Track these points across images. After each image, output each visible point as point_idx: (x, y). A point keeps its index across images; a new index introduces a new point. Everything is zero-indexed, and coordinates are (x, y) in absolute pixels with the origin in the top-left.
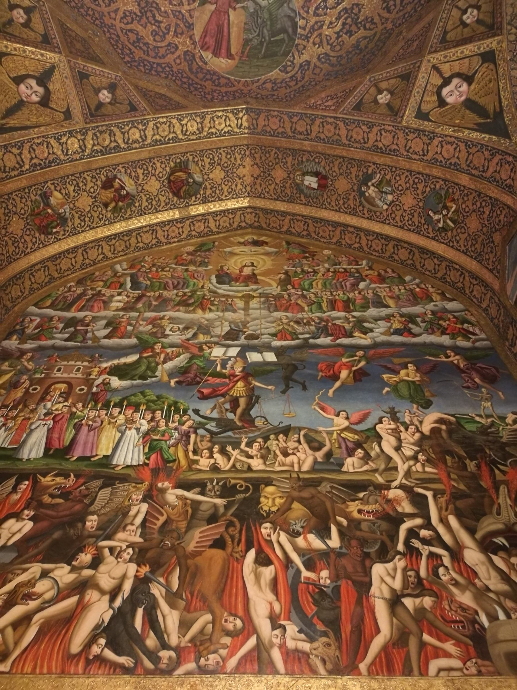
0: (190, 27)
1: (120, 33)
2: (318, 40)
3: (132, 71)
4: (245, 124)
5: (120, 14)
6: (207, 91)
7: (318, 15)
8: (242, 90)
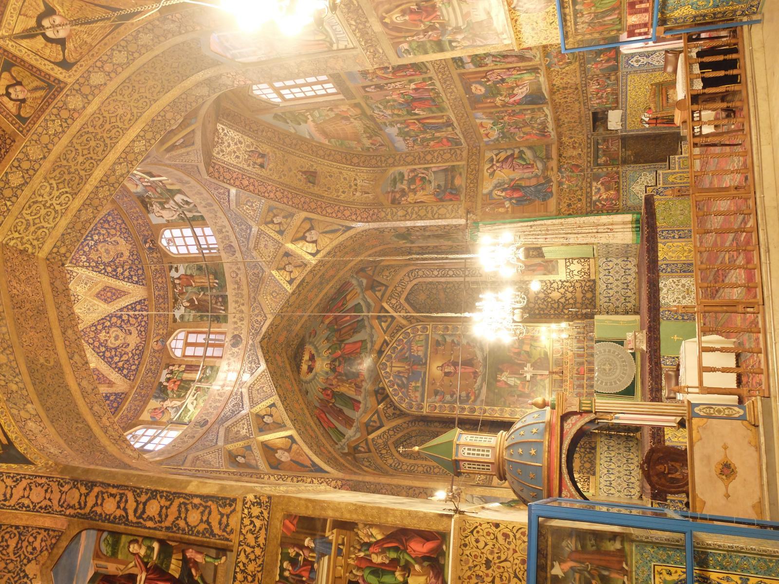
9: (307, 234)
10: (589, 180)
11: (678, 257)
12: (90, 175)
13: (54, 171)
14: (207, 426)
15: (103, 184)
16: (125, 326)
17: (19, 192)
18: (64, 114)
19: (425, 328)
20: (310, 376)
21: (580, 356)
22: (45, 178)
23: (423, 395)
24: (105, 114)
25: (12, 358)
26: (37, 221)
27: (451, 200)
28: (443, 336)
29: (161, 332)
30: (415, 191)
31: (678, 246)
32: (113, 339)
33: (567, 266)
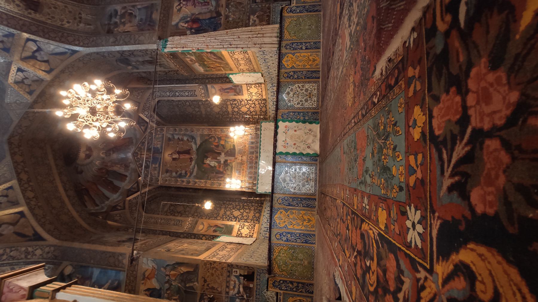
9: (37, 54)
10: (248, 14)
11: (304, 65)
19: (162, 130)
20: (88, 161)
21: (252, 148)
23: (159, 173)
27: (149, 30)
28: (173, 135)
30: (124, 24)
31: (304, 56)
33: (248, 90)
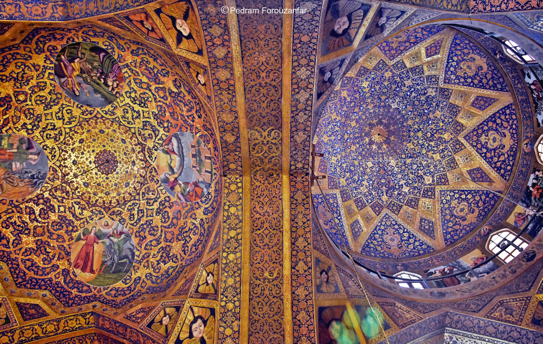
0: (68, 254)
1: (20, 263)
2: (146, 264)
3: (19, 290)
4: (92, 321)
5: (23, 250)
6: (71, 297)
7: (147, 249)
8: (96, 295)
12: (281, 111)
13: (252, 121)
14: (532, 263)
15: (296, 113)
16: (500, 129)
17: (238, 145)
18: (224, 86)
22: (249, 128)
24: (253, 68)
25: (238, 279)
26: (266, 155)
29: (529, 135)
32: (491, 141)
